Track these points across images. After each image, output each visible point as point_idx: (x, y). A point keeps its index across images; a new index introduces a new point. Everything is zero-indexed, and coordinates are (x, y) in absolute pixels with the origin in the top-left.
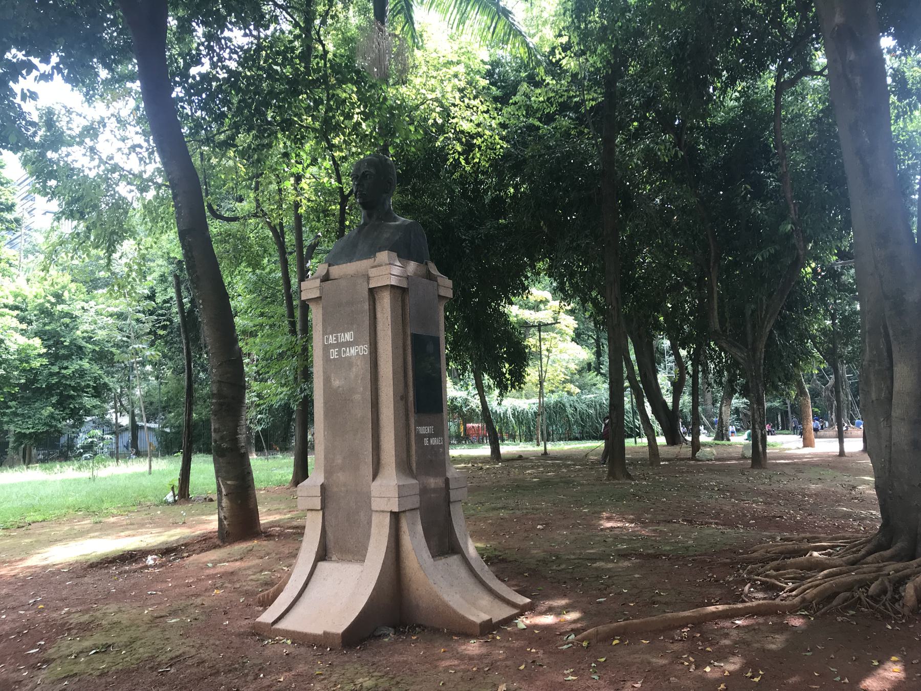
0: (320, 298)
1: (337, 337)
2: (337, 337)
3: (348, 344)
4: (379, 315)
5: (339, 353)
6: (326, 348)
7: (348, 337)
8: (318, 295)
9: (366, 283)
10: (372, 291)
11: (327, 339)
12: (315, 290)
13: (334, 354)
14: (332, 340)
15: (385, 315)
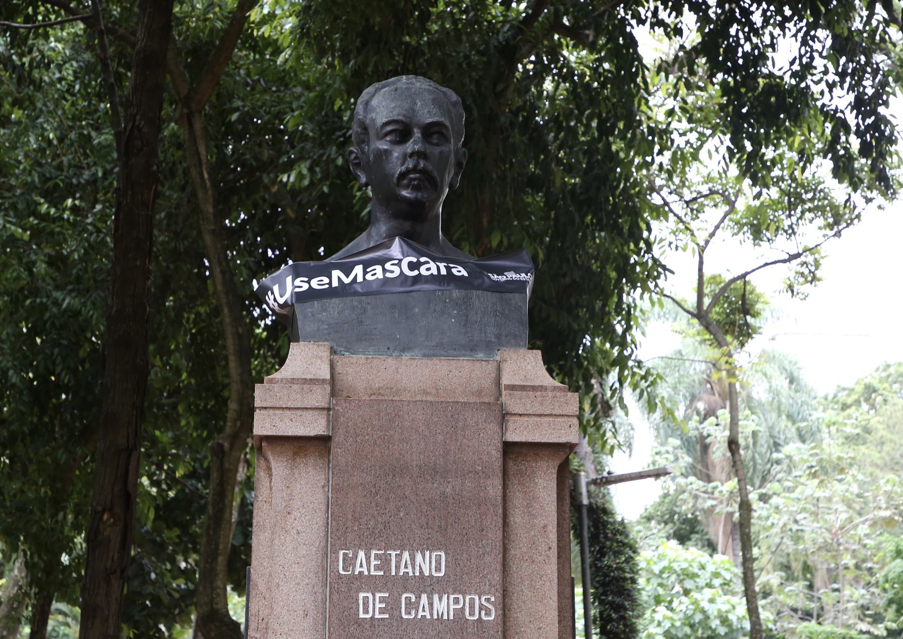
0: (322, 443)
1: (385, 563)
2: (385, 563)
3: (425, 585)
4: (517, 518)
5: (392, 606)
6: (339, 591)
7: (427, 563)
8: (315, 426)
9: (493, 427)
10: (510, 450)
11: (349, 562)
12: (308, 415)
13: (371, 606)
14: (365, 563)
15: (540, 522)
